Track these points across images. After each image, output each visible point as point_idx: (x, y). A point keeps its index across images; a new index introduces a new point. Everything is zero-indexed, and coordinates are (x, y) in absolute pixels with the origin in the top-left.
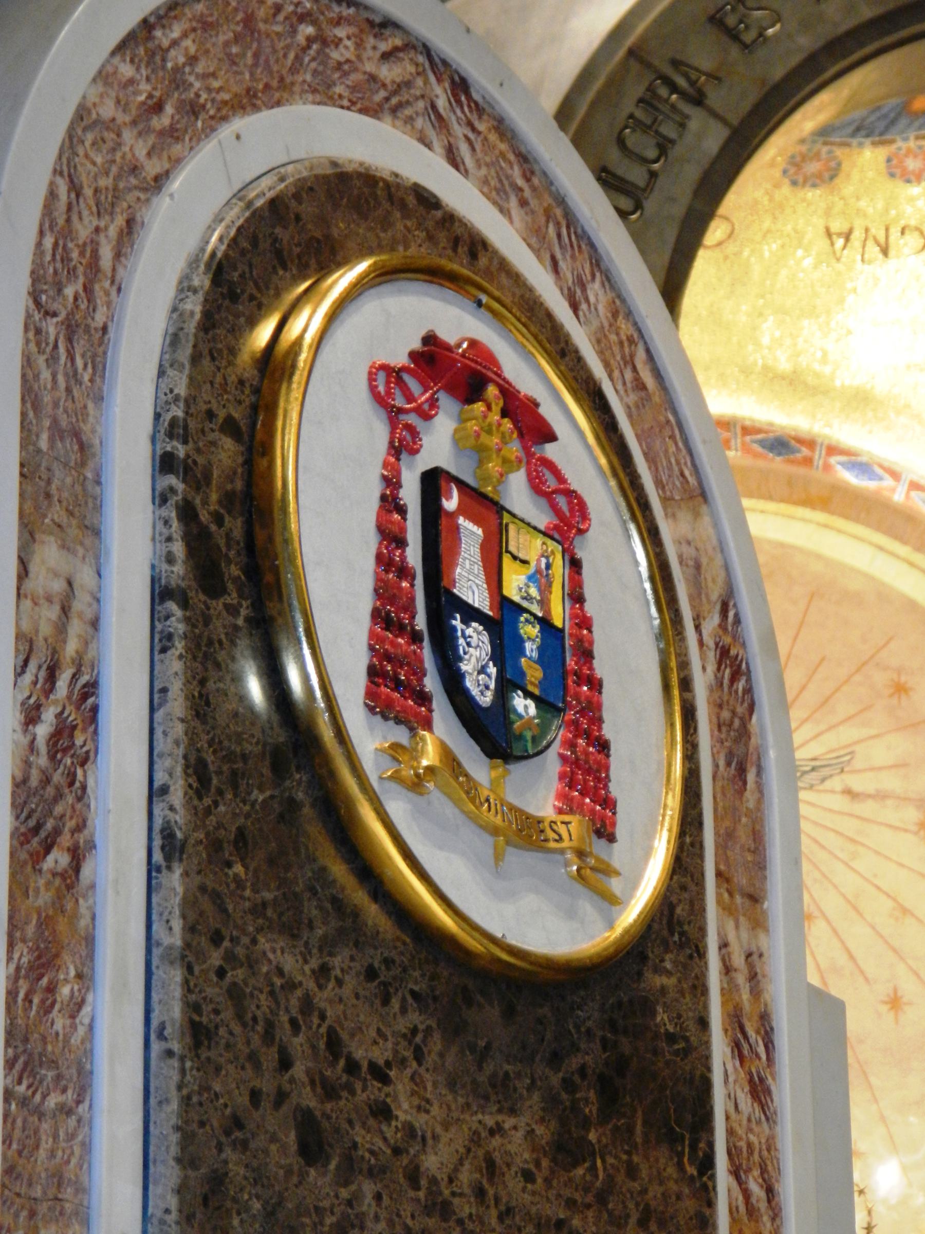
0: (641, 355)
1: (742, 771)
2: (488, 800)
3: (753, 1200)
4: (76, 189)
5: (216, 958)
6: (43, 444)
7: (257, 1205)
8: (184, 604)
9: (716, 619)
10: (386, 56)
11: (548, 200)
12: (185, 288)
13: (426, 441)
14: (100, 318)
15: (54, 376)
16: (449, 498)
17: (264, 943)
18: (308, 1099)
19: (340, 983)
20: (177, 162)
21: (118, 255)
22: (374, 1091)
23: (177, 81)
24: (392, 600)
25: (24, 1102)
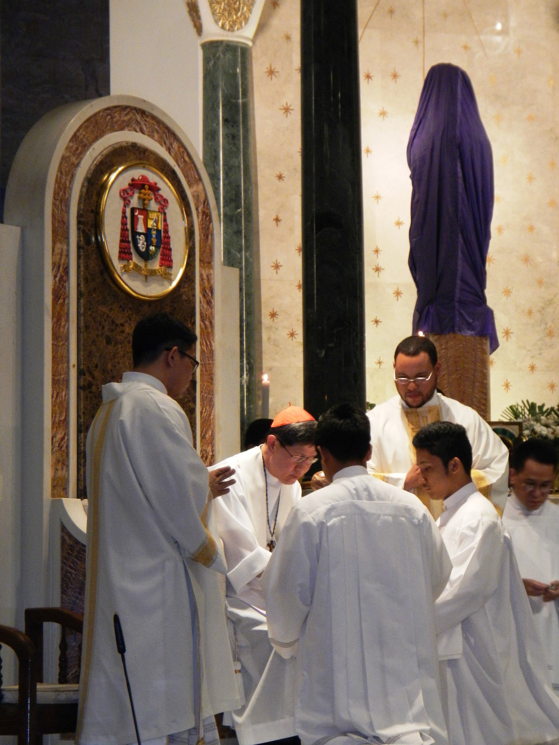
0: (185, 154)
1: (207, 237)
2: (144, 270)
3: (207, 325)
4: (62, 173)
5: (90, 313)
6: (57, 225)
8: (83, 249)
9: (202, 206)
10: (126, 115)
11: (164, 129)
12: (83, 186)
13: (132, 201)
14: (67, 196)
15: (58, 212)
16: (136, 212)
17: (99, 307)
18: (109, 333)
19: (114, 310)
20: (81, 159)
21: (70, 183)
22: (121, 328)
23: (82, 141)
24: (124, 237)
25: (56, 345)
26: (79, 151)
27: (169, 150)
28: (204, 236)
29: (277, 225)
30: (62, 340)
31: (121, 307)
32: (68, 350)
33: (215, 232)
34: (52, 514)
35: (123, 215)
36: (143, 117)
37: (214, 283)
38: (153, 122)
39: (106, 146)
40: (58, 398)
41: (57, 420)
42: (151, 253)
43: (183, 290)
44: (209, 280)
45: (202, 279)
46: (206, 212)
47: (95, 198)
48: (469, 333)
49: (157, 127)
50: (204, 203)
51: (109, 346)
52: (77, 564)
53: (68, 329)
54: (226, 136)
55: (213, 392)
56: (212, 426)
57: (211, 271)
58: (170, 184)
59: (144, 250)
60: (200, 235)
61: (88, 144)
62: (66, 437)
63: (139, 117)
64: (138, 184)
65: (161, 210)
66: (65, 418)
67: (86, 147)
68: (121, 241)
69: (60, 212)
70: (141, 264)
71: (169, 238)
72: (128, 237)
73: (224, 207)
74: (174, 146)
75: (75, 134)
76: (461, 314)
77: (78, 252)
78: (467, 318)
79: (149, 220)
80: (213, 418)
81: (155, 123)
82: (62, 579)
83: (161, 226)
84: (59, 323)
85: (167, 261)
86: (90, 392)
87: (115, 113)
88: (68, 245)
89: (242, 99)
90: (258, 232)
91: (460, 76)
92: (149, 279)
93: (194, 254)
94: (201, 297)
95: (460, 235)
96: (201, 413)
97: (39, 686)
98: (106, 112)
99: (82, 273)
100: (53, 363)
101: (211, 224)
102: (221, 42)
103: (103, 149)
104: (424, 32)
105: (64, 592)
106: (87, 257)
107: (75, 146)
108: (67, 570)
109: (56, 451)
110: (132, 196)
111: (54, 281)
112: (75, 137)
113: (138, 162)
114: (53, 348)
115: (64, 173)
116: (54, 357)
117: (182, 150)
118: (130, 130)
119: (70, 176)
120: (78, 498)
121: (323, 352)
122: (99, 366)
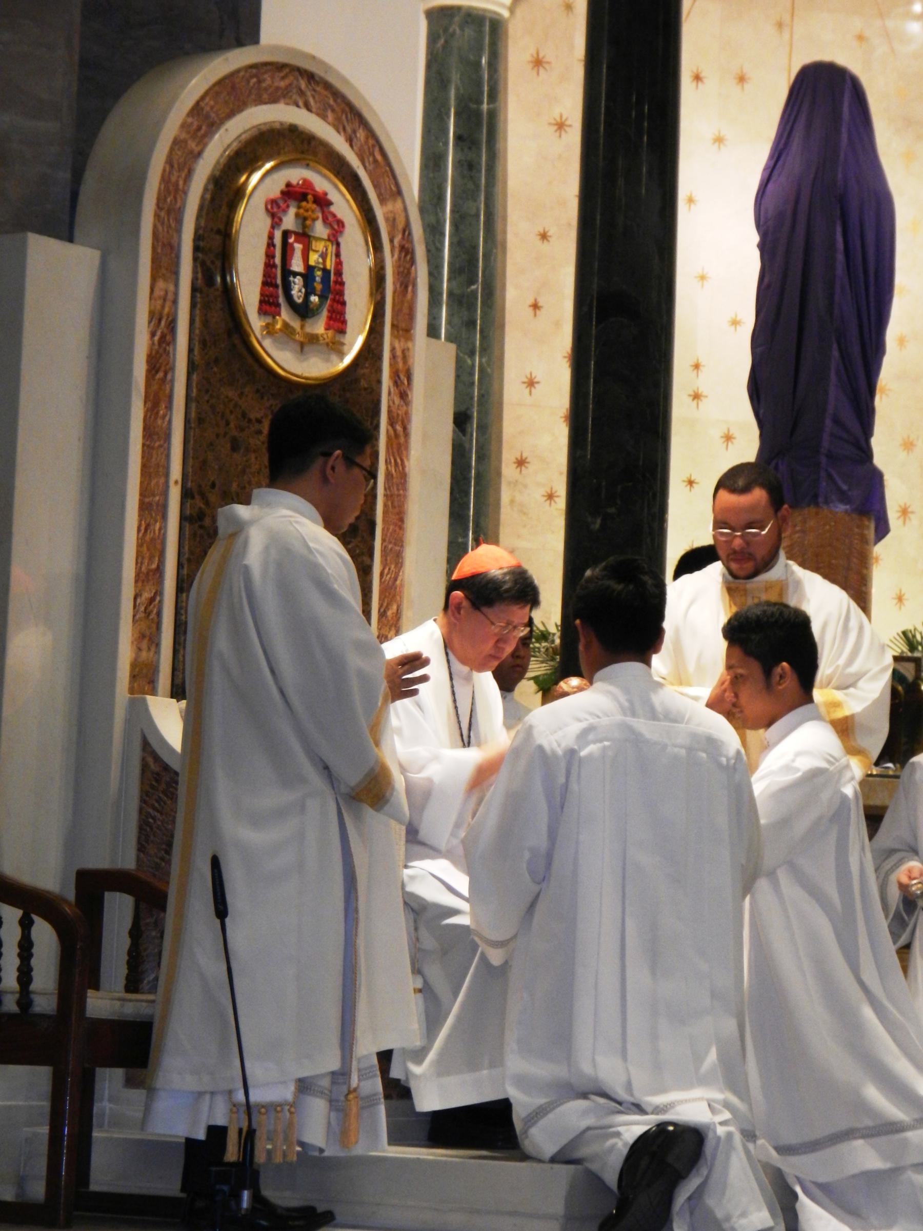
1: (406, 287)
2: (298, 333)
3: (398, 432)
4: (172, 166)
5: (206, 398)
6: (159, 250)
7: (217, 467)
8: (201, 292)
10: (283, 78)
11: (343, 105)
12: (206, 189)
13: (285, 219)
14: (178, 205)
15: (163, 228)
16: (291, 238)
18: (235, 433)
19: (247, 396)
20: (205, 145)
23: (207, 117)
24: (269, 277)
26: (202, 132)
27: (350, 141)
28: (401, 285)
29: (535, 315)
30: (159, 439)
31: (258, 391)
32: (168, 456)
33: (419, 280)
34: (128, 722)
35: (270, 241)
36: (310, 83)
37: (413, 364)
38: (326, 93)
39: (248, 126)
40: (149, 531)
41: (144, 569)
42: (311, 306)
43: (362, 371)
44: (405, 358)
45: (393, 356)
46: (406, 246)
47: (224, 210)
48: (841, 508)
49: (331, 102)
50: (404, 231)
51: (235, 455)
52: (165, 803)
53: (170, 422)
54: (458, 164)
55: (402, 541)
56: (398, 598)
57: (410, 344)
58: (349, 197)
59: (300, 301)
60: (394, 283)
61: (218, 121)
62: (158, 598)
63: (303, 84)
64: (296, 192)
65: (331, 238)
66: (158, 567)
67: (213, 126)
68: (265, 284)
69: (166, 230)
70: (296, 324)
71: (342, 284)
72: (275, 277)
73: (449, 280)
74: (358, 135)
75: (197, 103)
76: (830, 476)
77: (193, 297)
78: (840, 483)
79: (311, 253)
80: (402, 585)
81: (329, 95)
82: (141, 829)
83: (330, 264)
84: (155, 411)
85: (338, 321)
86: (201, 527)
87: (266, 73)
88: (177, 285)
89: (488, 104)
90: (502, 326)
91: (849, 81)
92: (306, 349)
93: (383, 315)
94: (391, 385)
95: (835, 346)
96: (382, 575)
97: (90, 993)
98: (250, 70)
99: (197, 332)
100: (142, 474)
101: (413, 268)
102: (458, 9)
103: (240, 131)
104: (793, 8)
105: (141, 848)
106: (207, 306)
107: (196, 124)
108: (149, 813)
109: (140, 620)
110: (285, 211)
111: (150, 342)
112: (196, 109)
113: (299, 156)
114: (143, 451)
115: (176, 166)
116: (144, 466)
117: (371, 142)
118: (287, 104)
119: (186, 170)
120: (172, 697)
121: (599, 521)
122: (217, 487)
